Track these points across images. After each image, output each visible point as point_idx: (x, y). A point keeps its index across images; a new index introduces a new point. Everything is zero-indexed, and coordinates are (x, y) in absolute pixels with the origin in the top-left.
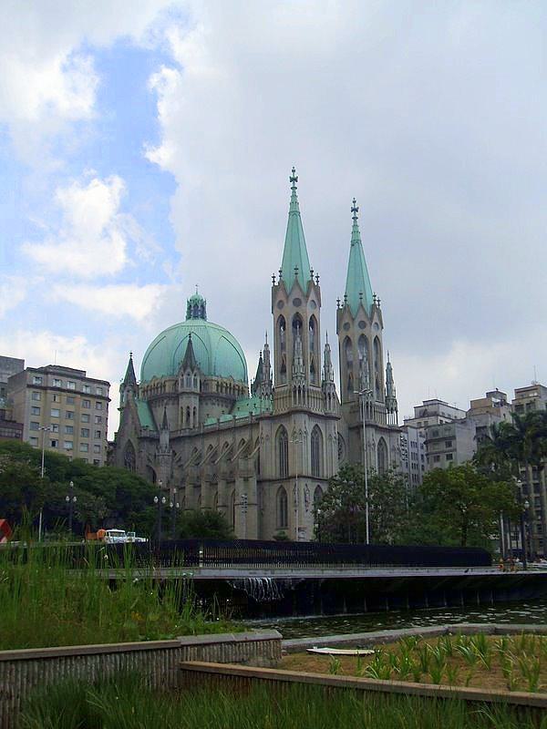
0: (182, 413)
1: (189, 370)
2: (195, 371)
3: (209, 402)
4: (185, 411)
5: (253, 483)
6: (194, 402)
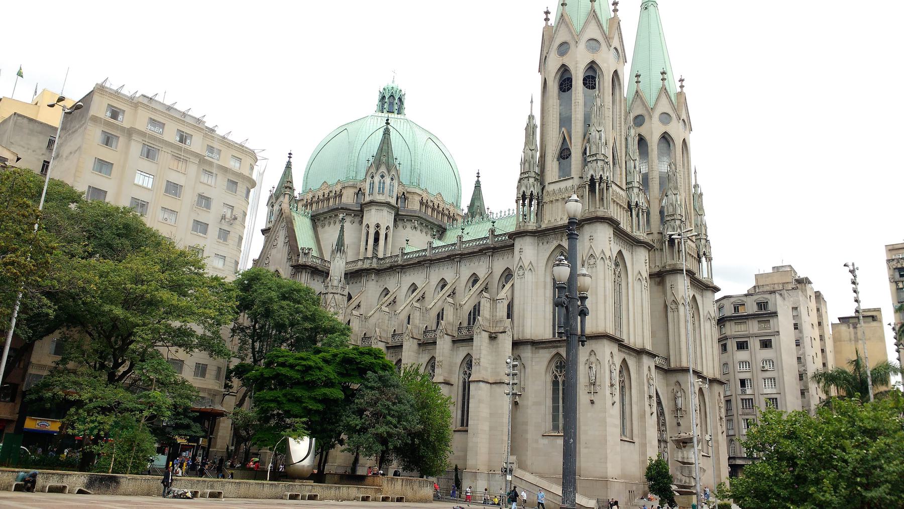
0: (368, 233)
1: (383, 169)
2: (393, 172)
3: (409, 225)
4: (372, 232)
5: (506, 343)
6: (385, 218)
